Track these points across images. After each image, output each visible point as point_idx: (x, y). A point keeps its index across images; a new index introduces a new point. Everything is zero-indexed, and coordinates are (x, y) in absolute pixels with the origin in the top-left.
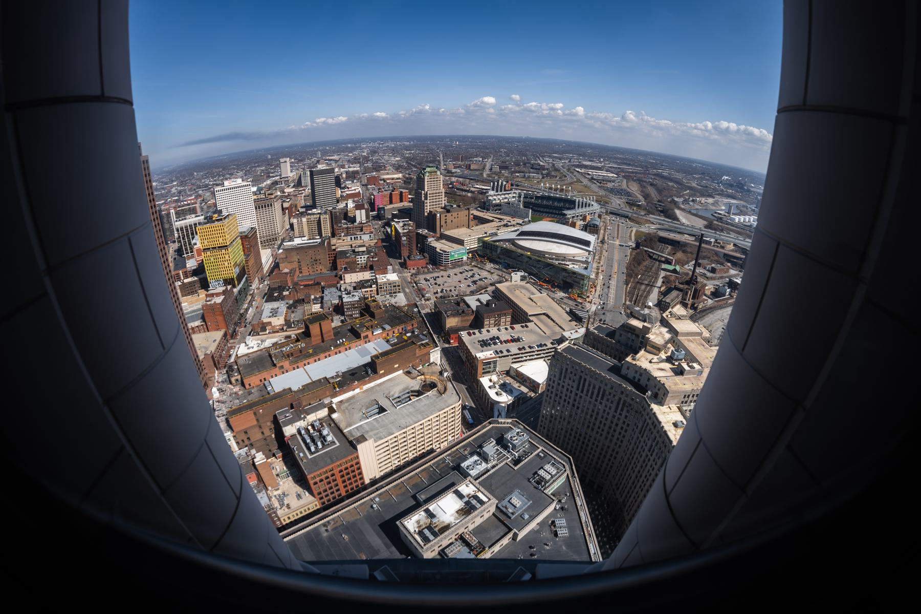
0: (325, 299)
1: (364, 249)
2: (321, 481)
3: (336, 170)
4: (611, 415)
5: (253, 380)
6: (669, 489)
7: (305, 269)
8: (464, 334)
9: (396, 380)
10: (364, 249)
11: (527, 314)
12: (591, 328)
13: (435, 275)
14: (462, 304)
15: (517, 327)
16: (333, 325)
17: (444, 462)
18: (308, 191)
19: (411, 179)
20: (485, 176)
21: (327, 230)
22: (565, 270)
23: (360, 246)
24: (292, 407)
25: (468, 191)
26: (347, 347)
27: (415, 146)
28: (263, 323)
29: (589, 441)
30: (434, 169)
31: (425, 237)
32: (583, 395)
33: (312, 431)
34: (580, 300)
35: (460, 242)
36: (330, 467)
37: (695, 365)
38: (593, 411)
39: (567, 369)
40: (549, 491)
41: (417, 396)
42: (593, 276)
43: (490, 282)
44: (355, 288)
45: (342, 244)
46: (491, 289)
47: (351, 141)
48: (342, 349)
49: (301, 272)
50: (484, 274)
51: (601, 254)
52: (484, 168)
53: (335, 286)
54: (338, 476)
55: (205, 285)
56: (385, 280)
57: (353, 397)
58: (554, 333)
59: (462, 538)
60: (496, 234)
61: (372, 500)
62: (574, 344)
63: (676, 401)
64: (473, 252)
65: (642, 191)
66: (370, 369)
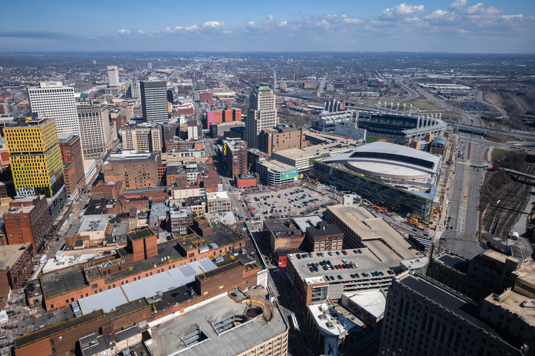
3: (168, 84)
5: (58, 301)
7: (132, 183)
8: (292, 256)
9: (219, 304)
10: (195, 166)
11: (360, 238)
12: (436, 258)
13: (265, 194)
14: (291, 225)
15: (350, 251)
16: (159, 241)
18: (138, 103)
19: (244, 97)
20: (319, 95)
21: (157, 145)
22: (404, 193)
23: (191, 163)
24: (101, 332)
25: (301, 111)
26: (171, 265)
27: (249, 63)
28: (80, 237)
30: (267, 88)
31: (257, 157)
34: (421, 226)
35: (291, 162)
39: (408, 304)
41: (242, 322)
42: (437, 200)
43: (321, 203)
44: (184, 204)
46: (321, 210)
47: (184, 55)
48: (165, 267)
49: (128, 186)
50: (315, 195)
51: (447, 175)
53: (163, 201)
56: (215, 197)
57: (172, 321)
58: (392, 261)
60: (328, 155)
62: (415, 275)
64: (305, 172)
65: (504, 104)
66: (193, 289)
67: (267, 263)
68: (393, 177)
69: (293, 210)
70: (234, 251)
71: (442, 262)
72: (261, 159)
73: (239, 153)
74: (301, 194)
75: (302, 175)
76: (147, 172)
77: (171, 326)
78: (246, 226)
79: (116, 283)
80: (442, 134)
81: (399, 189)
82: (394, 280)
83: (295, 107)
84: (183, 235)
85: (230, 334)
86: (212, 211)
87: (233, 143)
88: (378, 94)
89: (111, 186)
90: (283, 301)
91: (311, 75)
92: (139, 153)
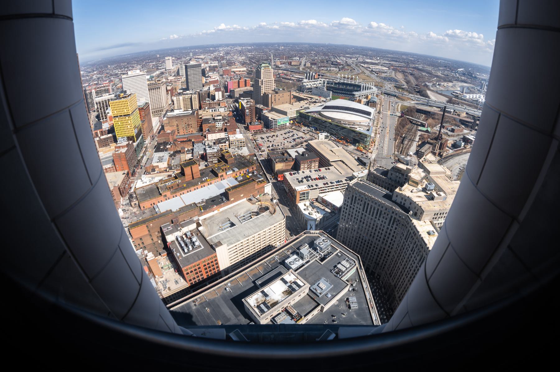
0: (195, 150)
1: (221, 118)
2: (192, 272)
4: (386, 228)
5: (146, 204)
6: (428, 277)
8: (287, 174)
10: (221, 118)
11: (329, 161)
12: (372, 170)
13: (268, 135)
14: (286, 155)
15: (323, 169)
16: (200, 168)
17: (274, 259)
18: (184, 79)
19: (252, 71)
20: (301, 69)
21: (196, 105)
22: (354, 131)
23: (218, 116)
24: (173, 223)
25: (290, 79)
26: (209, 183)
28: (153, 167)
29: (371, 245)
30: (267, 65)
32: (367, 215)
33: (185, 239)
35: (285, 113)
36: (197, 263)
37: (441, 193)
38: (374, 225)
39: (356, 197)
40: (344, 279)
41: (256, 215)
42: (373, 135)
43: (304, 139)
44: (214, 143)
45: (206, 114)
46: (305, 144)
48: (206, 184)
49: (178, 133)
50: (301, 134)
52: (300, 64)
53: (201, 142)
54: (203, 269)
55: (115, 140)
57: (213, 216)
58: (348, 173)
59: (286, 311)
60: (308, 108)
61: (225, 285)
62: (361, 181)
63: (429, 218)
64: (294, 119)
66: (225, 196)
67: (271, 179)
68: (349, 121)
69: (287, 144)
70: (249, 173)
71: (375, 172)
72: (264, 112)
73: (249, 108)
74: (291, 134)
75: (292, 122)
76: (190, 123)
77: (212, 219)
78: (256, 156)
79: (177, 194)
80: (375, 95)
81: (352, 129)
82: (348, 185)
83: (286, 77)
84: (215, 164)
85: (250, 223)
86: (233, 147)
87: (245, 101)
88: (337, 70)
89: (169, 133)
90: (281, 201)
91: (295, 56)
92: (185, 111)
